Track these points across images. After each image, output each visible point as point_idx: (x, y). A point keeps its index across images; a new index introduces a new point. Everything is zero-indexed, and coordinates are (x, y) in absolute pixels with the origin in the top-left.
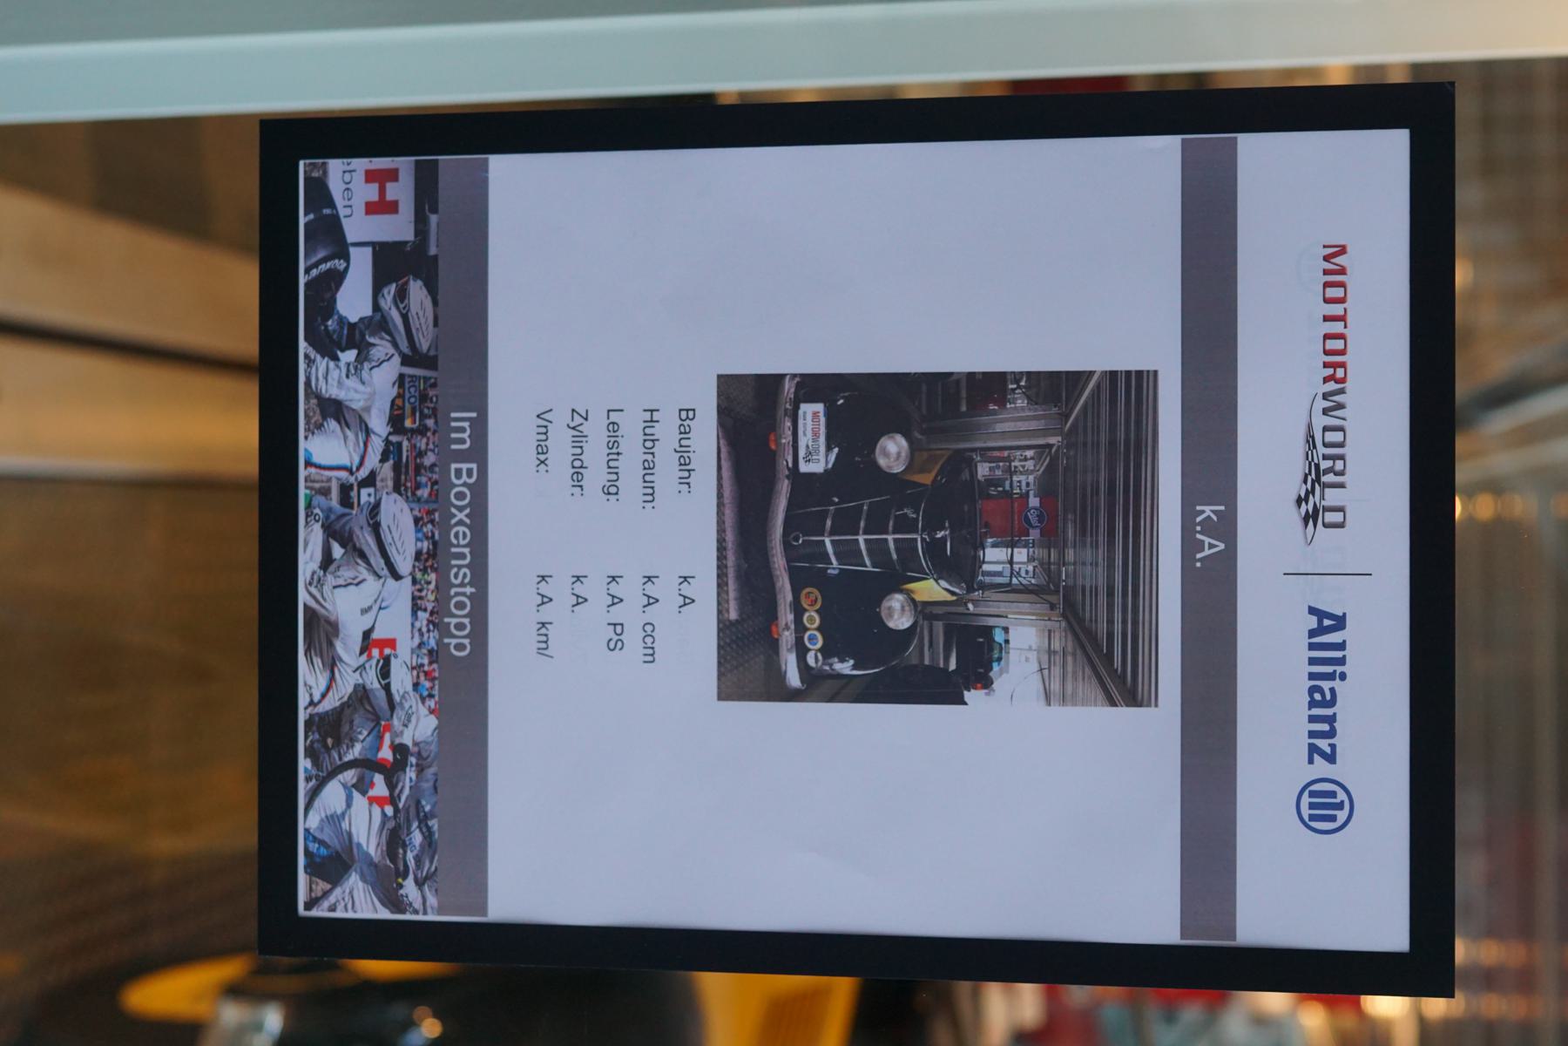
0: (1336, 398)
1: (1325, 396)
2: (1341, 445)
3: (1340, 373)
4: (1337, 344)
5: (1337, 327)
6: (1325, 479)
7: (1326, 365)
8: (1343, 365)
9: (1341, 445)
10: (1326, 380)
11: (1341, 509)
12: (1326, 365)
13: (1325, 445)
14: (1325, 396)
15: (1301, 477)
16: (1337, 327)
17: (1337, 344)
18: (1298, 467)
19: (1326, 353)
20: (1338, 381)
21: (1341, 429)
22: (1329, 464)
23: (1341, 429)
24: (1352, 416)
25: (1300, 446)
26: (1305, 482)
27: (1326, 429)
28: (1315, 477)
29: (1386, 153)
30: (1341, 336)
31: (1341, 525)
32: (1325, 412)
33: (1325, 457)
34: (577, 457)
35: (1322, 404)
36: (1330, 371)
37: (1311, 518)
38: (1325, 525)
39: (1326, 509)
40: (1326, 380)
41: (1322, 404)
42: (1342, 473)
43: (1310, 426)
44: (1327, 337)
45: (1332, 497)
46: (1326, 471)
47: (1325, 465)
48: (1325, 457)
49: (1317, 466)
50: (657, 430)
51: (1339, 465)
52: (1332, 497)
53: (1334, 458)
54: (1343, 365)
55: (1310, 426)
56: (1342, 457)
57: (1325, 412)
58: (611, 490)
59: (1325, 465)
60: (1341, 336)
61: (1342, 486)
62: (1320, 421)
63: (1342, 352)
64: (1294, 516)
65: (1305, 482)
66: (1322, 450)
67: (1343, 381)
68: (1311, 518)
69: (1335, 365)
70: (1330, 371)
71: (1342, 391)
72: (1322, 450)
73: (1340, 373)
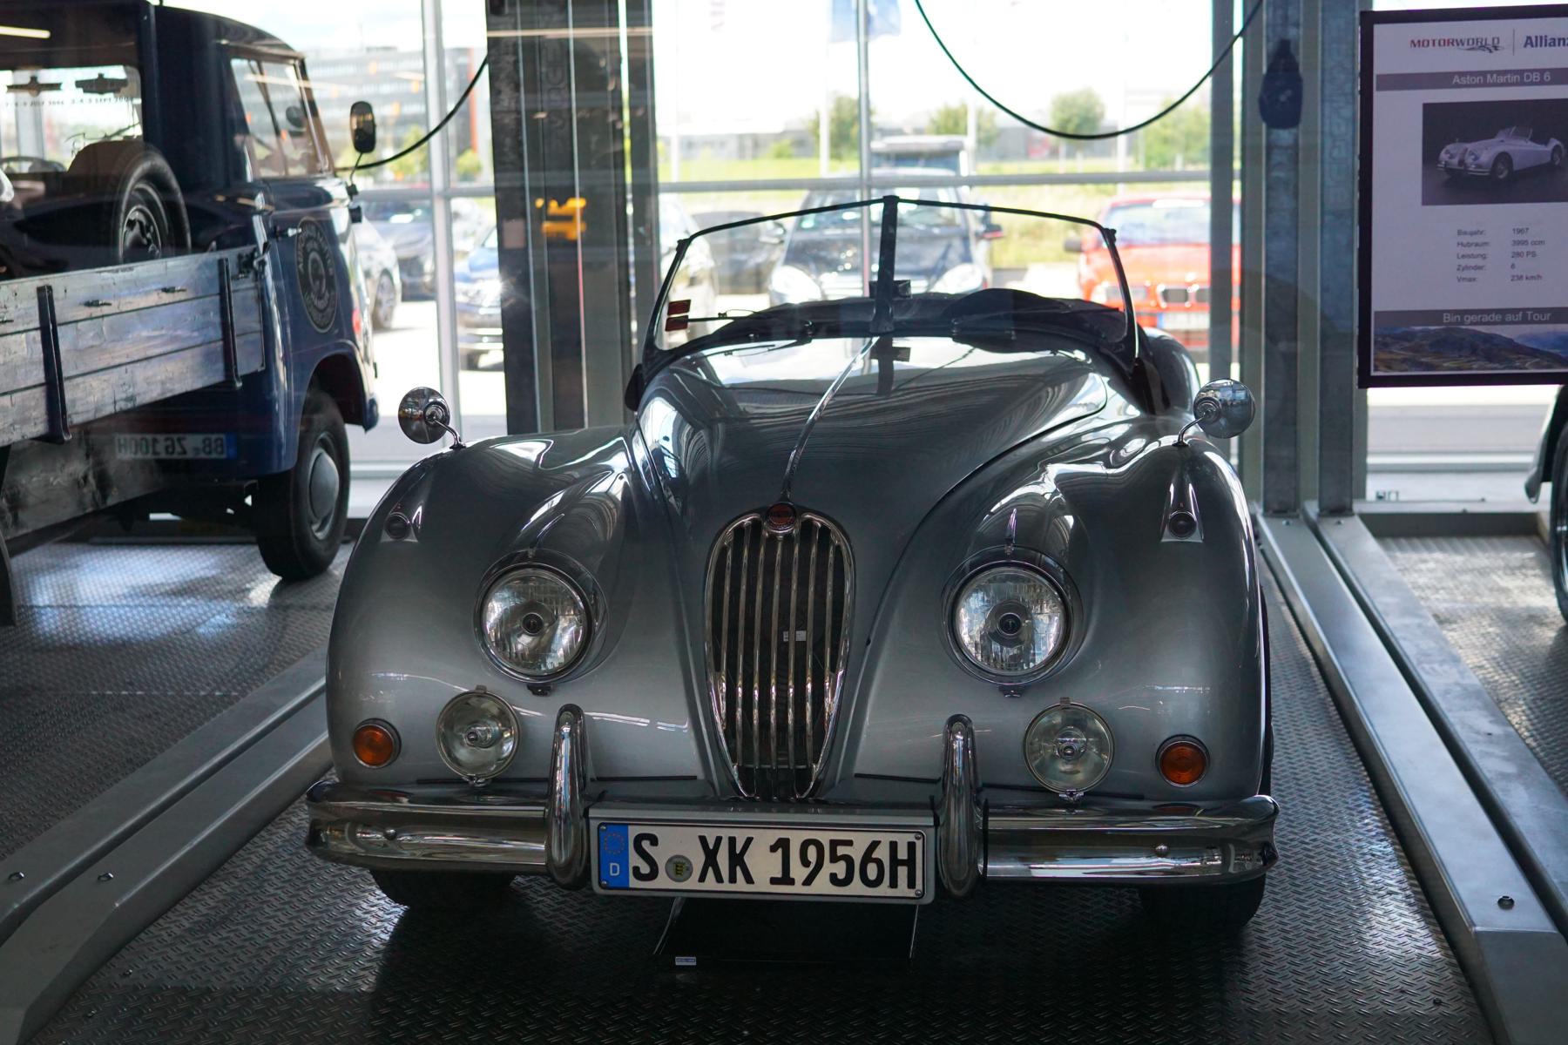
24: (1464, 36)
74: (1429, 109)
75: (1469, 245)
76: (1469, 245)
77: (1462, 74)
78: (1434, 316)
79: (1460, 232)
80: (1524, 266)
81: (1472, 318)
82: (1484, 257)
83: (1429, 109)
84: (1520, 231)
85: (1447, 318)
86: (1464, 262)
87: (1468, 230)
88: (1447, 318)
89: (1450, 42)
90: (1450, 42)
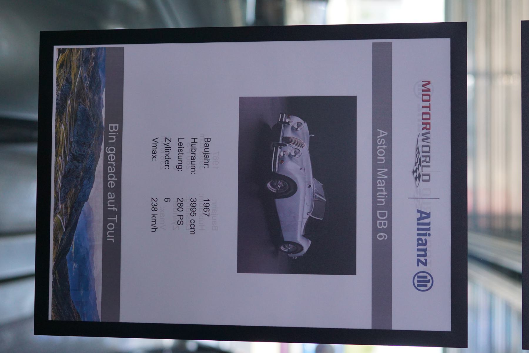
0: (428, 135)
1: (423, 135)
2: (429, 152)
3: (428, 126)
4: (428, 116)
5: (427, 110)
6: (422, 164)
7: (423, 124)
8: (429, 124)
9: (429, 152)
10: (423, 129)
11: (429, 175)
12: (423, 124)
13: (423, 152)
14: (423, 135)
15: (414, 163)
16: (427, 110)
17: (428, 116)
18: (413, 160)
19: (423, 119)
20: (427, 129)
21: (428, 146)
22: (424, 159)
23: (428, 146)
25: (414, 153)
26: (416, 165)
27: (423, 146)
28: (419, 163)
29: (444, 45)
30: (429, 113)
31: (429, 181)
32: (423, 140)
33: (423, 156)
34: (167, 155)
35: (422, 137)
36: (424, 126)
37: (418, 178)
38: (423, 181)
39: (423, 175)
40: (423, 129)
41: (422, 137)
42: (429, 162)
43: (417, 146)
44: (423, 114)
45: (425, 170)
46: (423, 162)
47: (423, 159)
48: (423, 156)
49: (420, 159)
50: (197, 146)
51: (428, 159)
52: (425, 170)
53: (426, 157)
54: (429, 124)
55: (417, 146)
56: (429, 156)
57: (423, 140)
58: (179, 167)
59: (423, 159)
60: (429, 113)
61: (429, 166)
62: (421, 143)
63: (429, 119)
64: (412, 178)
65: (416, 165)
66: (421, 154)
67: (429, 129)
68: (418, 178)
69: (426, 124)
70: (424, 126)
71: (429, 133)
72: (421, 154)
73: (428, 126)
74: (350, 102)
75: (194, 150)
76: (194, 150)
77: (389, 139)
78: (116, 114)
79: (208, 140)
80: (168, 211)
81: (112, 156)
82: (179, 167)
83: (350, 102)
84: (206, 207)
85: (113, 127)
86: (174, 146)
87: (211, 149)
88: (113, 127)
89: (426, 125)
90: (426, 125)
